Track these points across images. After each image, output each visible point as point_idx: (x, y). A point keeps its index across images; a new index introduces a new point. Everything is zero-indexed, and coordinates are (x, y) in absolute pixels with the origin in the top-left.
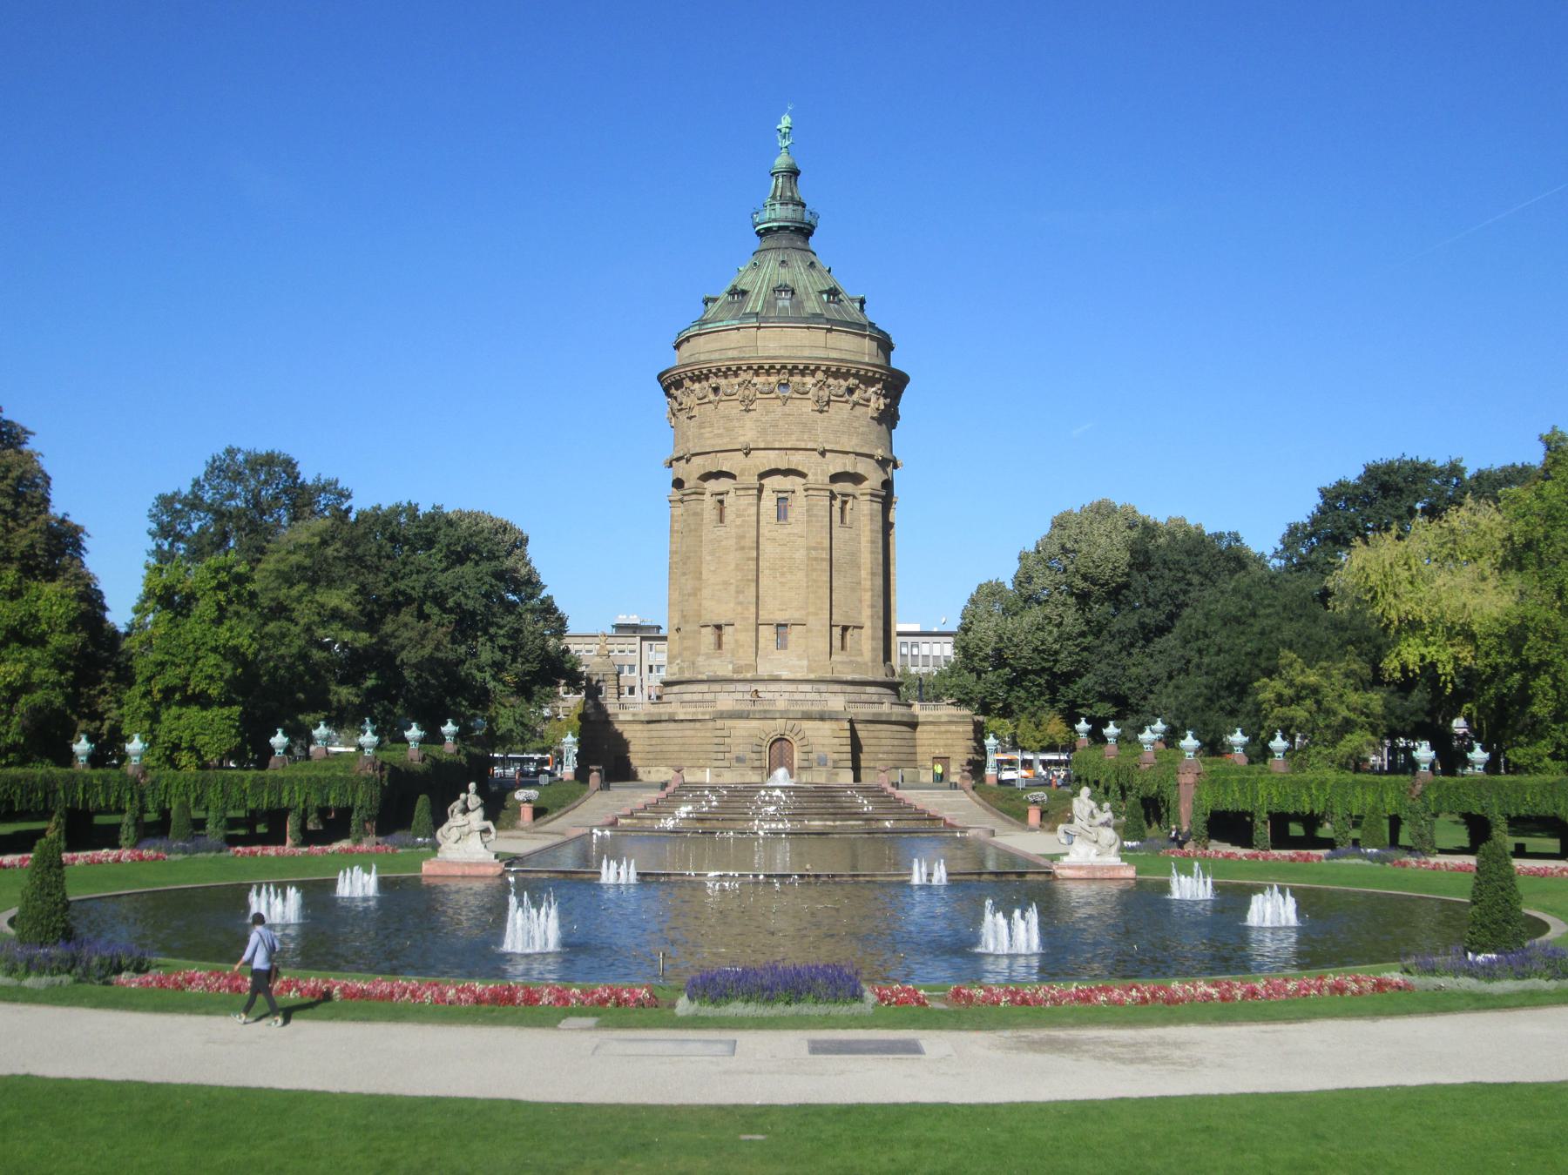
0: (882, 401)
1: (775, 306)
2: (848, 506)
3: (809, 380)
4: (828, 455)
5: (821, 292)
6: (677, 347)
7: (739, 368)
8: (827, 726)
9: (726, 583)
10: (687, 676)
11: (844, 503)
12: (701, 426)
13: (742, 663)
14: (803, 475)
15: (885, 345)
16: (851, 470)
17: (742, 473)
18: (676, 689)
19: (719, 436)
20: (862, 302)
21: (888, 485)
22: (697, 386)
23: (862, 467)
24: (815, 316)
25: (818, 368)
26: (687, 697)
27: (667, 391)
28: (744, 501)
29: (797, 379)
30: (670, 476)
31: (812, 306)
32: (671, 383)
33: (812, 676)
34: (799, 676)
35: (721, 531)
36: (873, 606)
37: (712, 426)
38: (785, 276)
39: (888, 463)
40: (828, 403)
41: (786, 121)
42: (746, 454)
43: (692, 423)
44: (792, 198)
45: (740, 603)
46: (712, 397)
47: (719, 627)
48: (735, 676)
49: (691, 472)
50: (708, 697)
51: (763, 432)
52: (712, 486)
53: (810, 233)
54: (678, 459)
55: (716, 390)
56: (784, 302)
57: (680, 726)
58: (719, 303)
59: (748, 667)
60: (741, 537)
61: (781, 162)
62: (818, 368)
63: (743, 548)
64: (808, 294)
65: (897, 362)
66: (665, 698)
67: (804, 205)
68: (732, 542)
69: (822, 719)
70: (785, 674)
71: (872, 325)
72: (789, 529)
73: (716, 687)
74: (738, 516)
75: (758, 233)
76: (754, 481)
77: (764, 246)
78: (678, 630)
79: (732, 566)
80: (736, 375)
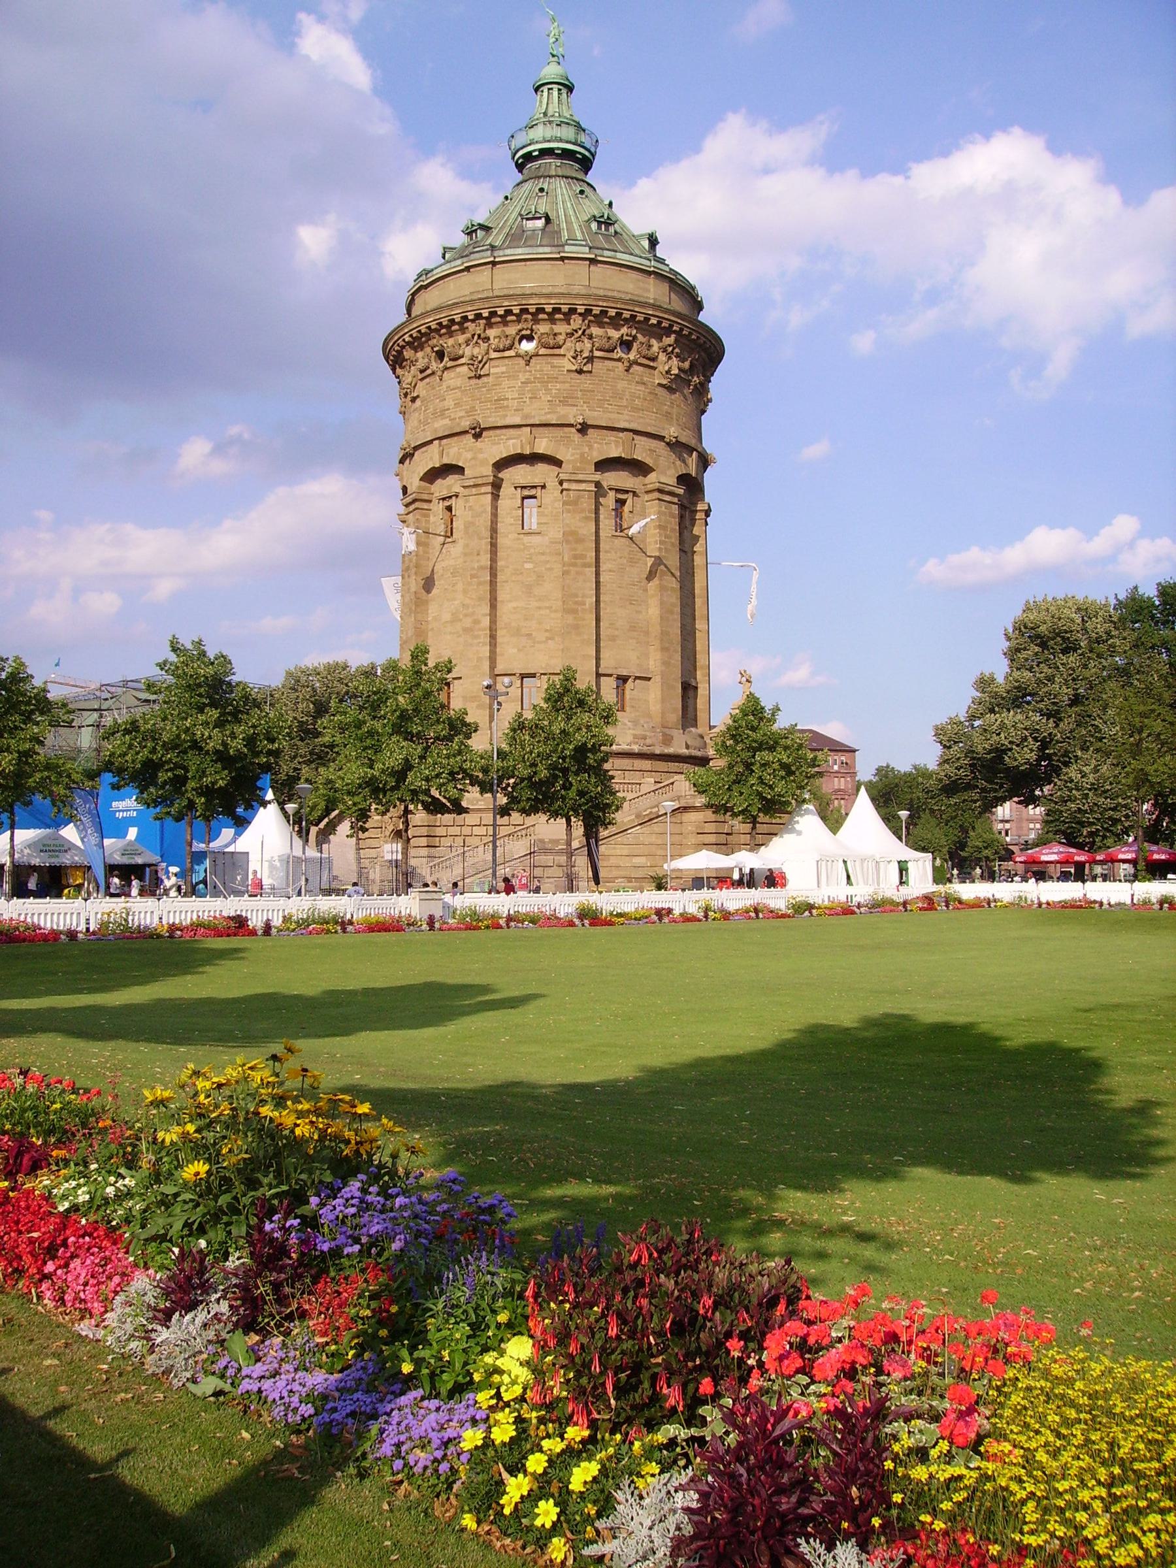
0: (675, 362)
2: (626, 508)
3: (562, 328)
4: (590, 431)
7: (465, 319)
11: (622, 502)
14: (558, 463)
22: (420, 354)
23: (642, 450)
25: (573, 311)
29: (543, 328)
36: (664, 649)
39: (689, 449)
40: (590, 359)
42: (477, 436)
46: (434, 366)
52: (442, 487)
55: (440, 355)
62: (573, 311)
76: (488, 471)
80: (463, 330)
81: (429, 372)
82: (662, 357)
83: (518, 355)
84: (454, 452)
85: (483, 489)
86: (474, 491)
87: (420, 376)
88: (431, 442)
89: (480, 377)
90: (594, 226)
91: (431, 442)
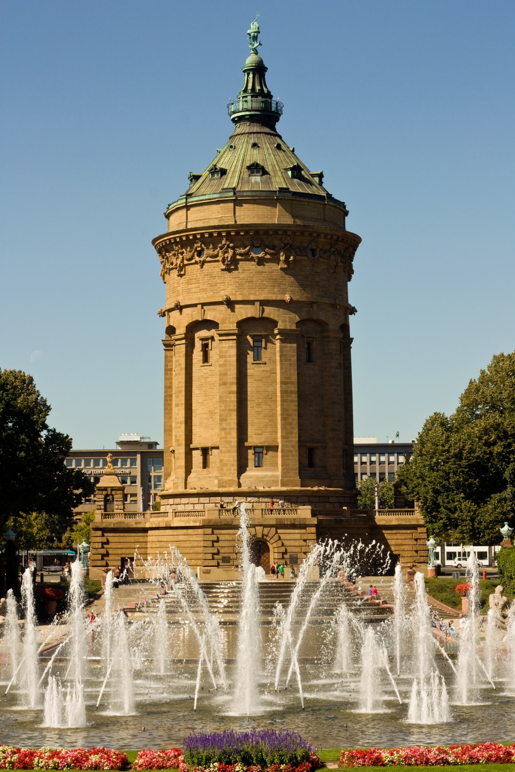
1: (248, 182)
5: (286, 170)
6: (168, 216)
7: (219, 233)
8: (297, 531)
9: (212, 413)
10: (181, 490)
12: (188, 283)
13: (226, 478)
14: (275, 323)
15: (341, 210)
16: (315, 317)
17: (224, 321)
18: (171, 501)
19: (204, 290)
20: (321, 176)
21: (345, 328)
23: (322, 316)
24: (282, 190)
26: (180, 508)
27: (160, 252)
28: (225, 344)
30: (164, 323)
31: (279, 181)
32: (165, 246)
33: (284, 489)
34: (273, 489)
35: (206, 370)
37: (198, 282)
38: (256, 156)
41: (253, 28)
43: (182, 280)
44: (262, 90)
45: (223, 429)
46: (197, 259)
47: (205, 451)
48: (221, 490)
49: (181, 321)
50: (199, 507)
51: (240, 287)
53: (278, 120)
54: (170, 310)
56: (256, 179)
57: (175, 532)
58: (201, 180)
59: (229, 483)
60: (223, 375)
61: (250, 60)
63: (225, 384)
64: (275, 171)
65: (351, 225)
66: (163, 509)
67: (271, 97)
68: (216, 379)
69: (293, 526)
70: (261, 489)
71: (329, 196)
72: (263, 368)
73: (202, 500)
74: (221, 357)
75: (233, 120)
76: (233, 327)
77: (239, 131)
78: (173, 451)
79: (217, 398)
81: (193, 261)
82: (333, 257)
83: (252, 259)
84: (211, 314)
85: (231, 337)
86: (224, 338)
87: (186, 262)
88: (195, 305)
89: (228, 270)
90: (290, 173)
91: (195, 305)
